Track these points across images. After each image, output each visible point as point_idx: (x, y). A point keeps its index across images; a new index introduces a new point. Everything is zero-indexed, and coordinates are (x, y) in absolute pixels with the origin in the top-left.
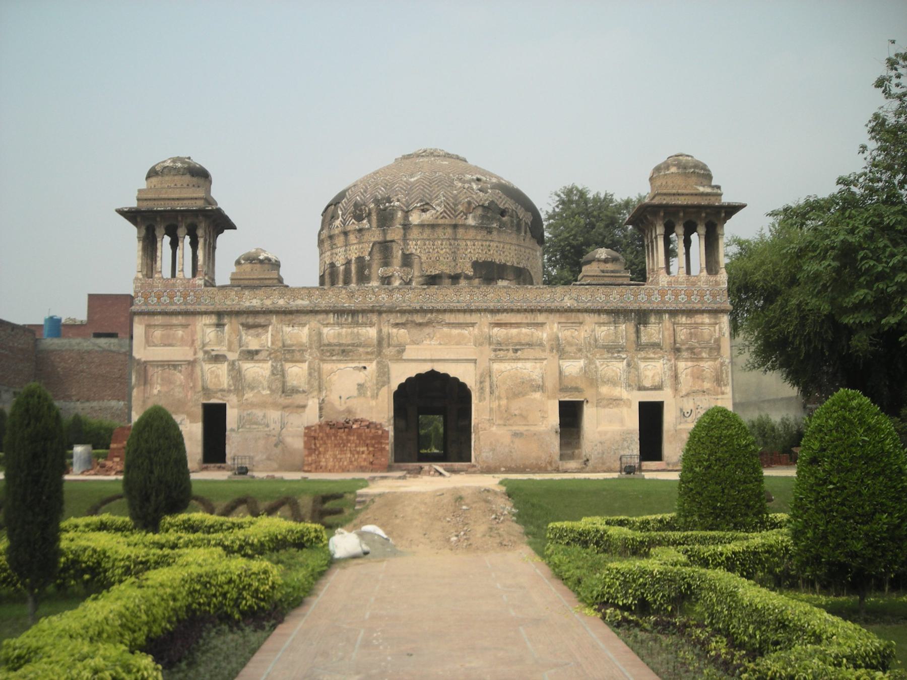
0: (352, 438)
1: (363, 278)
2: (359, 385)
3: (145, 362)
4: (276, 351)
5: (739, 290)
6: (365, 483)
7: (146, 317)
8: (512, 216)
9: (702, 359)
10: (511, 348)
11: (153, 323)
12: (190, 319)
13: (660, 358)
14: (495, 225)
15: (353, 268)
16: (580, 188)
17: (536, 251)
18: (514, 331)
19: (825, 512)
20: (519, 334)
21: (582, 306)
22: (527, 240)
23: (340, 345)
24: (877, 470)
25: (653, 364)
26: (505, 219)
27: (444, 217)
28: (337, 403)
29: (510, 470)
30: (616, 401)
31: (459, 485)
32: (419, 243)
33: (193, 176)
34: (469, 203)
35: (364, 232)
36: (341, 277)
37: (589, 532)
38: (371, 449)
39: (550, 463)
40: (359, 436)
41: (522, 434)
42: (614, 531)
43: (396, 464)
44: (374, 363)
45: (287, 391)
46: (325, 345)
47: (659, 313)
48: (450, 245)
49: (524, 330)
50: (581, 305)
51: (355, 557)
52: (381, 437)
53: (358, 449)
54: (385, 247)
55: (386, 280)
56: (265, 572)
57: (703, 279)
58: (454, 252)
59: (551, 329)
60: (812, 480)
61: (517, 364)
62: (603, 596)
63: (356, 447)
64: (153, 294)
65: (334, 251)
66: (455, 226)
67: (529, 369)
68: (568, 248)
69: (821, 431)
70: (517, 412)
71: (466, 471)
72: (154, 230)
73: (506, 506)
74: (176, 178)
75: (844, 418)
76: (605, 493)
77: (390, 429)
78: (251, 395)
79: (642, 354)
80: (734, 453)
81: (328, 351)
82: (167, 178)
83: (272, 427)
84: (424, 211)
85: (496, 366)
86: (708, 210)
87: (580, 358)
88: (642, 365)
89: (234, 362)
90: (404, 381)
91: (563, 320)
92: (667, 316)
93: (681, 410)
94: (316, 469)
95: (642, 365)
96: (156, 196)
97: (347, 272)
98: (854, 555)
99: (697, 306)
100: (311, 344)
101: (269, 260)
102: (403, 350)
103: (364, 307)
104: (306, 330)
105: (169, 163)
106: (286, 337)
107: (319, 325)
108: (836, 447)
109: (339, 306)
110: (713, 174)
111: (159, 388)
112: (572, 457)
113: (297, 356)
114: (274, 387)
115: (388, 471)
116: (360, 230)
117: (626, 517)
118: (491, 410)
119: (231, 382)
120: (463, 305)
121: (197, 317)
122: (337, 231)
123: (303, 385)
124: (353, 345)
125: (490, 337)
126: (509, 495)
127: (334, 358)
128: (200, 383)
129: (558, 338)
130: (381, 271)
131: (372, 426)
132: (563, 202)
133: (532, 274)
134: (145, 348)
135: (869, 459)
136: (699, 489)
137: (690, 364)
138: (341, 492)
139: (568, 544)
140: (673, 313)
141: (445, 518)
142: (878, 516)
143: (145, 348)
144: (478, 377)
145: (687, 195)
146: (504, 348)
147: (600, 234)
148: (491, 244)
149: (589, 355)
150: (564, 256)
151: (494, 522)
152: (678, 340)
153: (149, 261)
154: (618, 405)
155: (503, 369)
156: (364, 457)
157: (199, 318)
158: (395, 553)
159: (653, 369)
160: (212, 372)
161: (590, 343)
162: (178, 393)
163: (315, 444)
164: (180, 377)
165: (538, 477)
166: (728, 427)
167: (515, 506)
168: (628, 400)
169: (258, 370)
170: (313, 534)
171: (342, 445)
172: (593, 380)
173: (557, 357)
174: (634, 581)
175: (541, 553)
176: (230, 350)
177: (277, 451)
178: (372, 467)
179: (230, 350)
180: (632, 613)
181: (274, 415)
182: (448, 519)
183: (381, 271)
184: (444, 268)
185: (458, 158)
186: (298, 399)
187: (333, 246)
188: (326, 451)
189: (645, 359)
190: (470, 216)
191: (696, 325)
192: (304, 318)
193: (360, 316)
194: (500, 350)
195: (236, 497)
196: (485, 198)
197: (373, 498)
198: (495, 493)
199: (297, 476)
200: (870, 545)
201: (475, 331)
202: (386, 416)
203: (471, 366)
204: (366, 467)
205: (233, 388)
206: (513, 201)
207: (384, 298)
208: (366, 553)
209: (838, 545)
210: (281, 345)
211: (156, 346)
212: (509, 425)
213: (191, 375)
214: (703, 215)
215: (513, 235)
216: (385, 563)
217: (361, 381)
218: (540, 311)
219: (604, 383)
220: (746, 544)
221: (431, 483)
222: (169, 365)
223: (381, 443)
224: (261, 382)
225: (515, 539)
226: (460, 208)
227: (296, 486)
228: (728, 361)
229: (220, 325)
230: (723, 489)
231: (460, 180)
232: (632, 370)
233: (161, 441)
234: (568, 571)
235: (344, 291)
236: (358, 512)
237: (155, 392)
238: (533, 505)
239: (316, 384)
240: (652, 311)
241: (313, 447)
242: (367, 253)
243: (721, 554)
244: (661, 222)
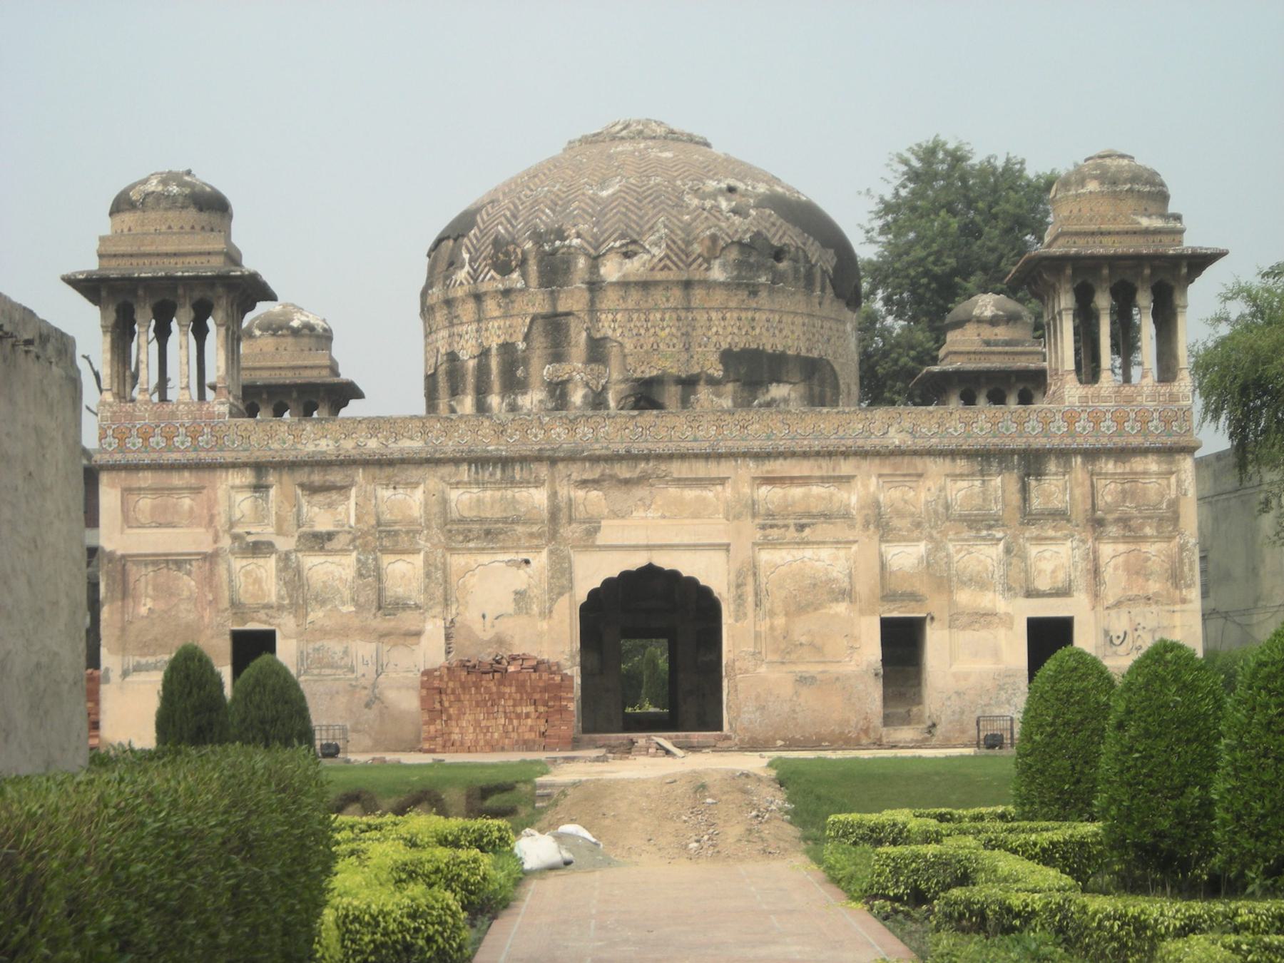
0: (507, 690)
1: (513, 384)
2: (516, 593)
3: (123, 557)
4: (364, 534)
5: (1244, 390)
6: (544, 768)
7: (123, 474)
8: (795, 260)
9: (1144, 539)
10: (791, 522)
11: (135, 485)
12: (206, 476)
13: (1066, 538)
14: (763, 279)
15: (494, 363)
16: (951, 146)
17: (844, 323)
18: (797, 492)
19: (1130, 785)
20: (806, 497)
21: (921, 443)
22: (827, 302)
23: (481, 521)
24: (1192, 735)
25: (1054, 548)
26: (783, 265)
27: (665, 267)
28: (477, 627)
29: (791, 745)
30: (984, 618)
31: (700, 768)
32: (619, 316)
33: (201, 210)
34: (714, 238)
35: (513, 297)
36: (470, 380)
37: (884, 827)
38: (542, 709)
39: (866, 731)
40: (521, 687)
41: (813, 678)
42: (914, 824)
43: (587, 737)
44: (545, 553)
45: (386, 605)
46: (453, 521)
47: (1064, 454)
48: (679, 319)
49: (816, 490)
50: (919, 441)
51: (552, 868)
52: (559, 687)
53: (519, 710)
54: (554, 326)
55: (558, 392)
56: (475, 861)
57: (1147, 391)
58: (687, 334)
59: (866, 486)
60: (1117, 749)
61: (810, 549)
62: (871, 887)
63: (514, 706)
64: (134, 432)
65: (455, 330)
66: (687, 285)
67: (826, 560)
68: (924, 281)
69: (1129, 689)
70: (803, 639)
71: (715, 748)
72: (132, 312)
73: (777, 799)
74: (170, 214)
75: (1156, 675)
76: (937, 778)
77: (575, 672)
78: (321, 614)
79: (1033, 531)
80: (1090, 715)
81: (459, 532)
82: (152, 215)
83: (359, 675)
84: (627, 255)
85: (765, 556)
86: (1157, 262)
87: (918, 540)
88: (1033, 550)
89: (287, 556)
90: (598, 584)
91: (886, 471)
92: (1079, 459)
93: (1106, 633)
94: (444, 747)
95: (1033, 550)
96: (134, 249)
97: (482, 371)
98: (1160, 835)
99: (1136, 441)
100: (428, 520)
101: (310, 328)
102: (597, 530)
103: (525, 450)
104: (419, 494)
105: (153, 186)
106: (383, 508)
107: (442, 485)
108: (1144, 709)
109: (479, 450)
110: (1172, 190)
111: (150, 604)
112: (906, 720)
113: (404, 541)
114: (362, 600)
115: (573, 749)
116: (507, 293)
117: (949, 810)
118: (757, 636)
119: (283, 592)
120: (705, 446)
121: (218, 473)
122: (460, 293)
123: (414, 594)
124: (504, 520)
125: (754, 503)
126: (782, 782)
127: (471, 545)
128: (227, 594)
129: (877, 505)
130: (548, 371)
131: (542, 667)
132: (914, 176)
133: (837, 368)
134: (122, 532)
135: (1182, 723)
136: (1039, 766)
137: (1122, 547)
138: (510, 780)
139: (855, 843)
140: (1091, 455)
141: (679, 817)
142: (1188, 790)
143: (122, 532)
144: (733, 577)
145: (1118, 233)
146: (780, 522)
147: (992, 250)
148: (757, 316)
149: (934, 533)
150: (918, 300)
151: (755, 822)
152: (1100, 503)
153: (121, 370)
154: (988, 625)
155: (779, 562)
156: (529, 726)
157: (221, 474)
158: (608, 863)
159: (1054, 558)
160: (248, 574)
161: (936, 512)
162: (187, 613)
163: (441, 702)
164: (188, 584)
165: (839, 755)
166: (1082, 678)
167: (789, 800)
168: (1007, 614)
169: (332, 568)
170: (496, 834)
171: (490, 704)
172: (944, 581)
173: (876, 538)
174: (906, 866)
175: (819, 861)
176: (280, 532)
177: (371, 714)
178: (545, 741)
179: (280, 532)
180: (904, 903)
181: (364, 650)
182: (684, 818)
183: (548, 371)
184: (668, 364)
185: (691, 139)
186: (408, 620)
187: (452, 321)
188: (461, 713)
189: (1039, 540)
190: (716, 264)
191: (1134, 477)
192: (414, 473)
193: (517, 468)
194: (772, 527)
195: (341, 791)
196: (742, 227)
197: (564, 790)
198: (759, 779)
199: (426, 759)
200: (1180, 823)
201: (727, 492)
202: (567, 650)
203: (720, 556)
204: (534, 742)
205: (286, 602)
206: (798, 230)
207: (560, 436)
208: (567, 863)
209: (1143, 825)
210: (373, 522)
211: (142, 526)
212: (792, 658)
213: (209, 580)
214: (1147, 271)
215: (799, 297)
216: (598, 874)
217: (521, 586)
218: (845, 454)
219: (964, 583)
220: (1070, 832)
221: (653, 766)
222: (167, 562)
223: (561, 699)
224: (338, 591)
225: (787, 845)
226: (697, 248)
227: (431, 774)
228: (1193, 541)
229: (259, 488)
230: (1073, 767)
231: (696, 192)
232: (1015, 561)
233: (280, 707)
234: (843, 869)
235: (487, 423)
236: (540, 811)
237: (143, 610)
238: (819, 798)
239: (439, 593)
240: (1050, 451)
241: (438, 706)
242: (521, 337)
243: (1035, 844)
244: (1068, 286)
